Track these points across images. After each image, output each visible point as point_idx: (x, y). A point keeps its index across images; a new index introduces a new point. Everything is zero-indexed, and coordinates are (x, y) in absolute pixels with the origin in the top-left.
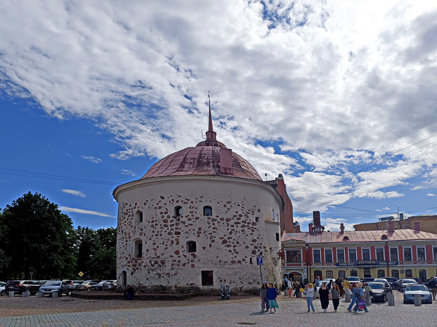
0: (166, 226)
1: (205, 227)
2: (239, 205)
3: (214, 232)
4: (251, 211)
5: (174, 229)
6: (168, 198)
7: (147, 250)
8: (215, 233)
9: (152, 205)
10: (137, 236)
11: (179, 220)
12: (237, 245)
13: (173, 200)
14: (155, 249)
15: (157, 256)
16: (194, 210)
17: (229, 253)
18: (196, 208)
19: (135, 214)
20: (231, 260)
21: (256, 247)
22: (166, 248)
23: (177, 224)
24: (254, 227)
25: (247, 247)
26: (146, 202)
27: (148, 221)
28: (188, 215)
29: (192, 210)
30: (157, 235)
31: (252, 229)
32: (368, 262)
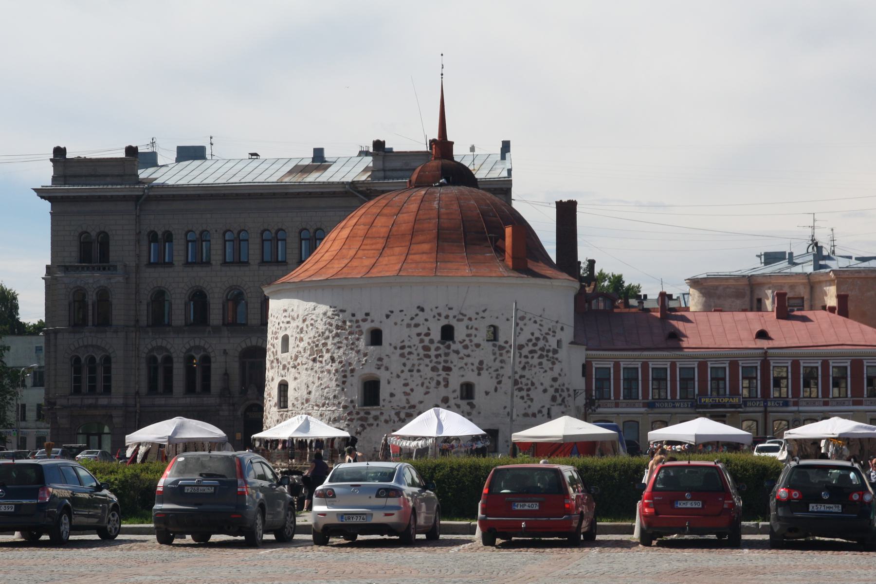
0: (428, 356)
1: (489, 359)
2: (535, 322)
3: (502, 368)
4: (552, 330)
5: (442, 361)
6: (431, 310)
7: (392, 395)
8: (502, 369)
9: (403, 320)
10: (370, 370)
11: (449, 347)
12: (532, 388)
13: (439, 315)
14: (406, 394)
15: (409, 405)
16: (473, 332)
17: (521, 400)
18: (476, 329)
19: (364, 331)
20: (523, 412)
21: (557, 390)
22: (427, 393)
23: (447, 355)
24: (556, 356)
25: (545, 391)
26: (389, 313)
27: (393, 345)
28: (464, 341)
29: (470, 332)
30: (411, 371)
31: (552, 360)
32: (722, 400)
